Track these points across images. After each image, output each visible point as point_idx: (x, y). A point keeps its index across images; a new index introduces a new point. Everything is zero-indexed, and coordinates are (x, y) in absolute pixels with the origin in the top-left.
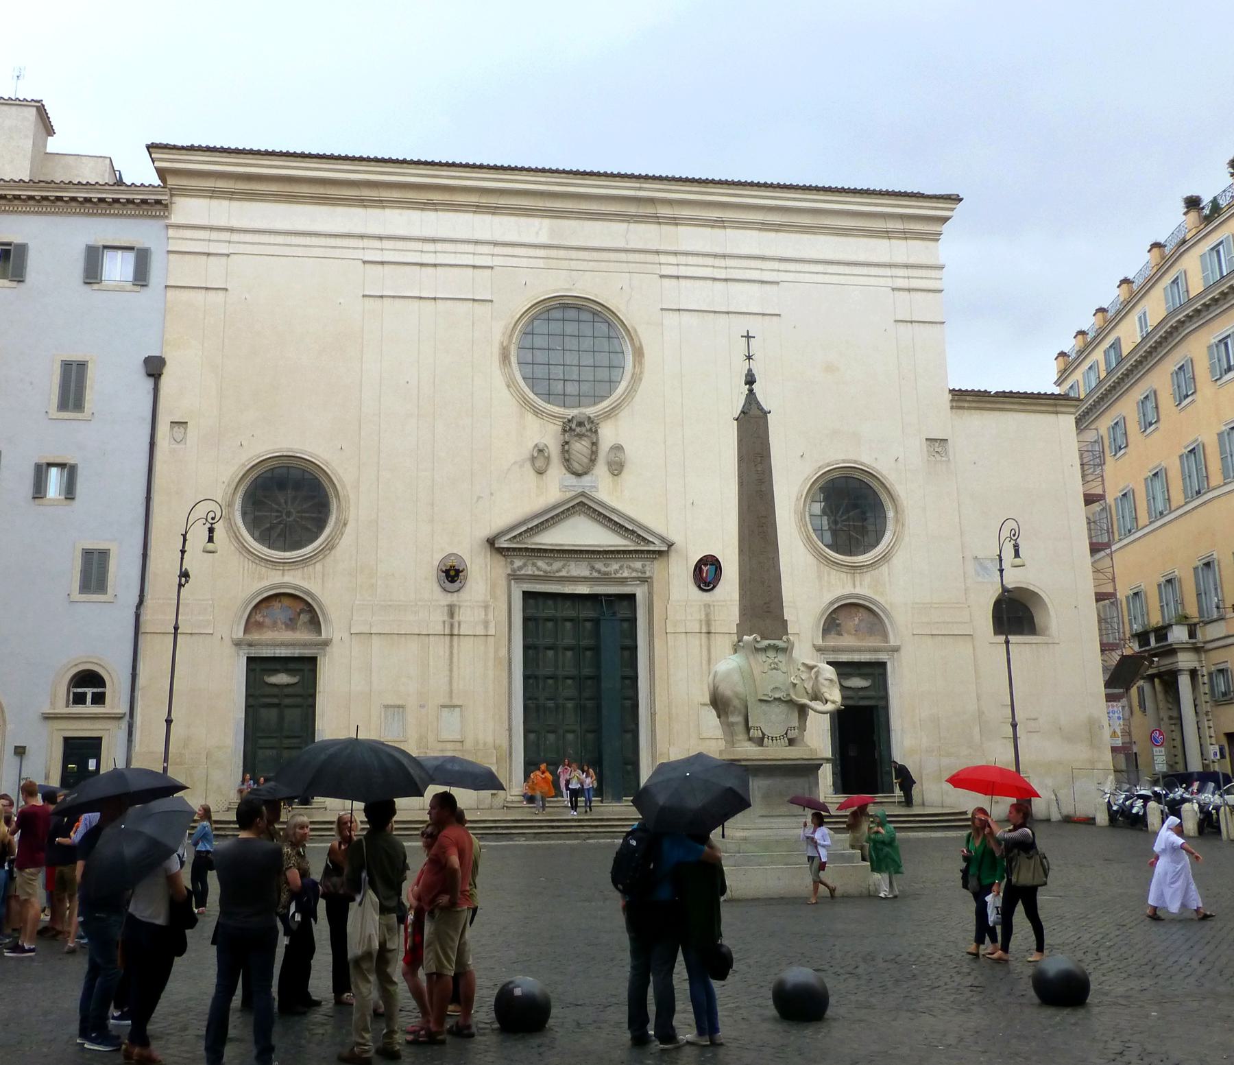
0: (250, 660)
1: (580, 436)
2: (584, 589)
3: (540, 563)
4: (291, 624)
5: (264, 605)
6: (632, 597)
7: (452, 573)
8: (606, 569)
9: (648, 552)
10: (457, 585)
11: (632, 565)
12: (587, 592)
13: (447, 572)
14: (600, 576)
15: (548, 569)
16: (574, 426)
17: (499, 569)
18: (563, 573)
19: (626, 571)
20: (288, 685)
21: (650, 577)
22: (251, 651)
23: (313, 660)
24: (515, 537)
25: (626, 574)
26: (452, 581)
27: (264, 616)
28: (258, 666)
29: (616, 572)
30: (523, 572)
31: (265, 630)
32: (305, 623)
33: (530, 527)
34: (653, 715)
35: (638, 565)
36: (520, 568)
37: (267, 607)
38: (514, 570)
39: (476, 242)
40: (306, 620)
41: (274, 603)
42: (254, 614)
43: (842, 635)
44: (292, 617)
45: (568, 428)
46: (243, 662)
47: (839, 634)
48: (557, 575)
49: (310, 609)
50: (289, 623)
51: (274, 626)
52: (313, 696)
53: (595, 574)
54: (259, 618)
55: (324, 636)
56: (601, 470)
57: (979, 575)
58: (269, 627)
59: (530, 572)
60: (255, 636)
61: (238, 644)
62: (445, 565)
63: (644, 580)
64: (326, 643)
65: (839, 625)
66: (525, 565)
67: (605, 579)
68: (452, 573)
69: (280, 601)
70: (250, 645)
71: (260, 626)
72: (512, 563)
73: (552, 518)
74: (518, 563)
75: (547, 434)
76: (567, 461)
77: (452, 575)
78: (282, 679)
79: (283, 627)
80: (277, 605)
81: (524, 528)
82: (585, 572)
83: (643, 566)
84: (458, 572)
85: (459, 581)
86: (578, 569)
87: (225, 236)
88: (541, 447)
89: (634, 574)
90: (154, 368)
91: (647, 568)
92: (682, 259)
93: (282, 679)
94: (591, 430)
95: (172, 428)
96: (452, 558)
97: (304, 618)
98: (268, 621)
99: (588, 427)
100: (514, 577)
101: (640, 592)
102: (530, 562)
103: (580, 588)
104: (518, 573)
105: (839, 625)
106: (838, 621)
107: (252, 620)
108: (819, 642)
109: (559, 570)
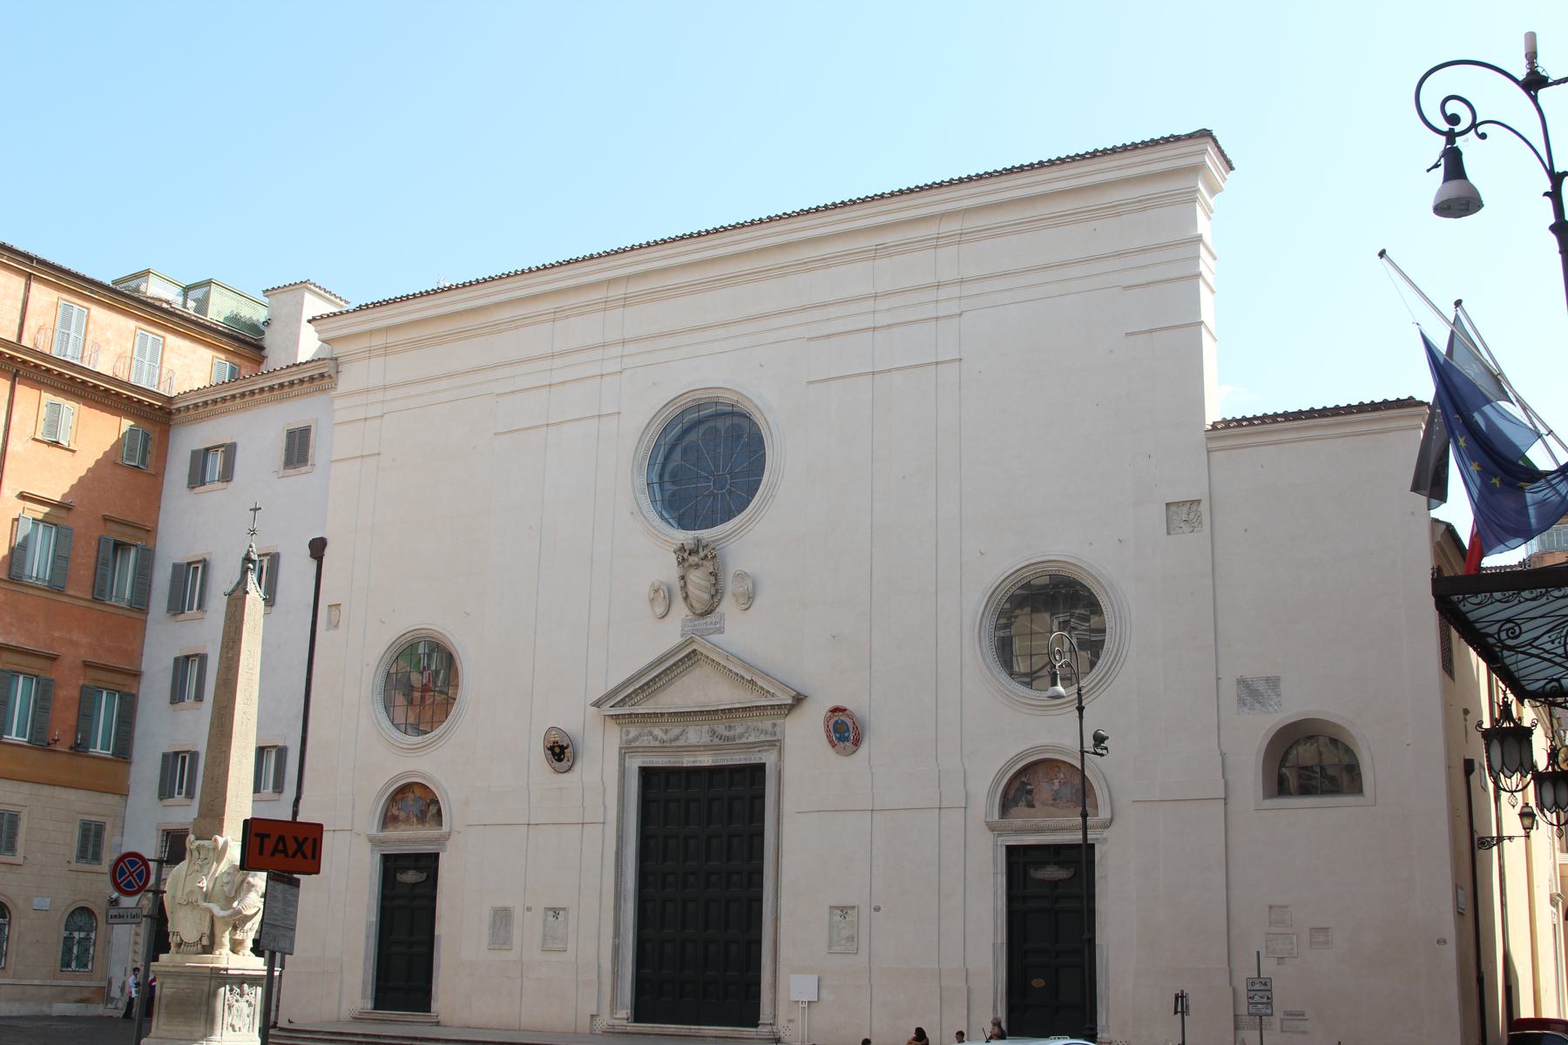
0: (388, 860)
1: (697, 566)
2: (706, 760)
3: (657, 731)
4: (422, 818)
5: (400, 796)
6: (760, 769)
7: (557, 750)
8: (731, 733)
9: (773, 707)
10: (565, 764)
11: (760, 725)
12: (709, 764)
13: (551, 749)
14: (721, 742)
15: (665, 738)
16: (686, 555)
17: (614, 738)
18: (681, 742)
19: (753, 735)
20: (414, 885)
21: (779, 741)
22: (383, 848)
23: (436, 856)
24: (622, 702)
25: (751, 739)
26: (560, 760)
27: (398, 809)
28: (392, 865)
29: (741, 736)
30: (637, 744)
31: (400, 823)
32: (433, 815)
33: (637, 687)
34: (776, 919)
35: (767, 724)
36: (636, 739)
37: (402, 799)
38: (630, 742)
39: (604, 345)
40: (435, 811)
41: (408, 794)
42: (391, 806)
43: (1033, 806)
44: (423, 808)
45: (680, 560)
46: (378, 857)
47: (1031, 805)
48: (674, 744)
49: (438, 802)
50: (420, 815)
51: (407, 820)
52: (434, 898)
53: (716, 741)
54: (395, 811)
55: (445, 828)
56: (728, 606)
57: (1245, 704)
58: (403, 821)
59: (645, 744)
60: (393, 833)
61: (374, 842)
62: (549, 742)
63: (772, 744)
64: (447, 837)
65: (1030, 792)
66: (640, 735)
67: (727, 743)
68: (557, 750)
69: (413, 792)
70: (382, 842)
71: (395, 819)
72: (628, 733)
73: (664, 672)
74: (633, 732)
75: (666, 569)
76: (686, 598)
77: (559, 752)
78: (410, 877)
79: (415, 819)
80: (411, 796)
81: (632, 690)
82: (706, 739)
83: (774, 725)
84: (563, 748)
85: (566, 759)
86: (696, 734)
87: (379, 396)
88: (657, 585)
89: (762, 738)
90: (318, 548)
91: (778, 729)
92: (832, 312)
93: (410, 877)
94: (706, 556)
95: (330, 613)
96: (554, 733)
97: (433, 809)
98: (402, 815)
99: (702, 554)
100: (626, 751)
101: (768, 758)
102: (646, 731)
103: (700, 759)
104: (633, 745)
105: (1030, 792)
106: (1029, 787)
107: (389, 814)
108: (996, 817)
109: (677, 738)
